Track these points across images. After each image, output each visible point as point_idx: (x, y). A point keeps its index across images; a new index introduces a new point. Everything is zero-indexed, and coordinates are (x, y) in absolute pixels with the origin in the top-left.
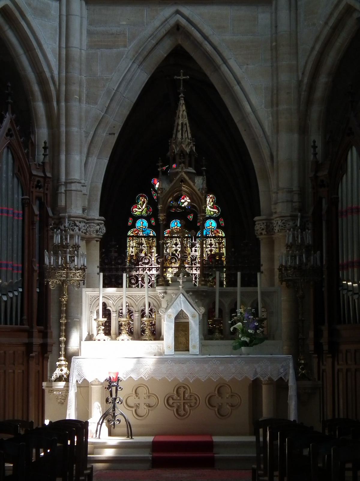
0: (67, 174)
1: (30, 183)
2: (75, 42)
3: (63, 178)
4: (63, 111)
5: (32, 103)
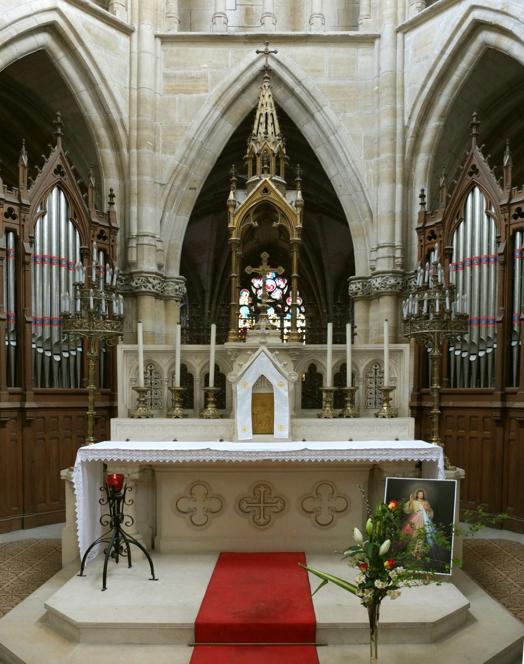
0: (139, 227)
1: (90, 233)
3: (134, 232)
5: (99, 150)
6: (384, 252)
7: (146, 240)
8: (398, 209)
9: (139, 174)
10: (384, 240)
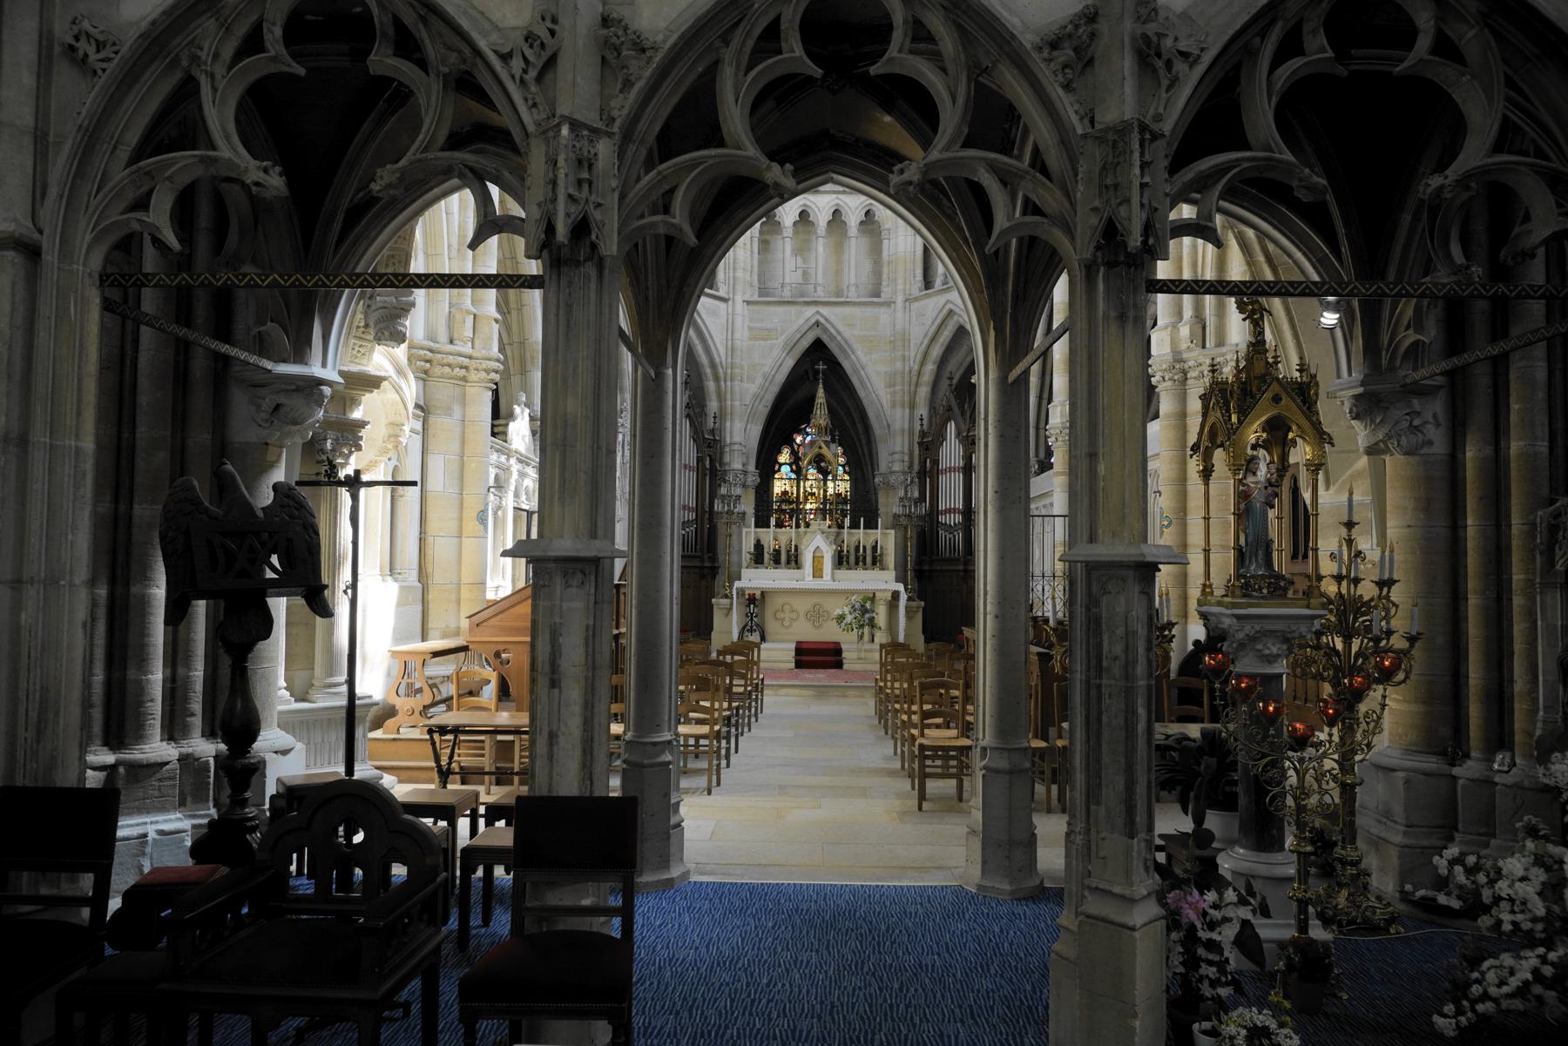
0: (731, 437)
2: (738, 335)
4: (729, 389)
6: (897, 457)
7: (736, 447)
8: (906, 426)
9: (732, 400)
10: (898, 449)
